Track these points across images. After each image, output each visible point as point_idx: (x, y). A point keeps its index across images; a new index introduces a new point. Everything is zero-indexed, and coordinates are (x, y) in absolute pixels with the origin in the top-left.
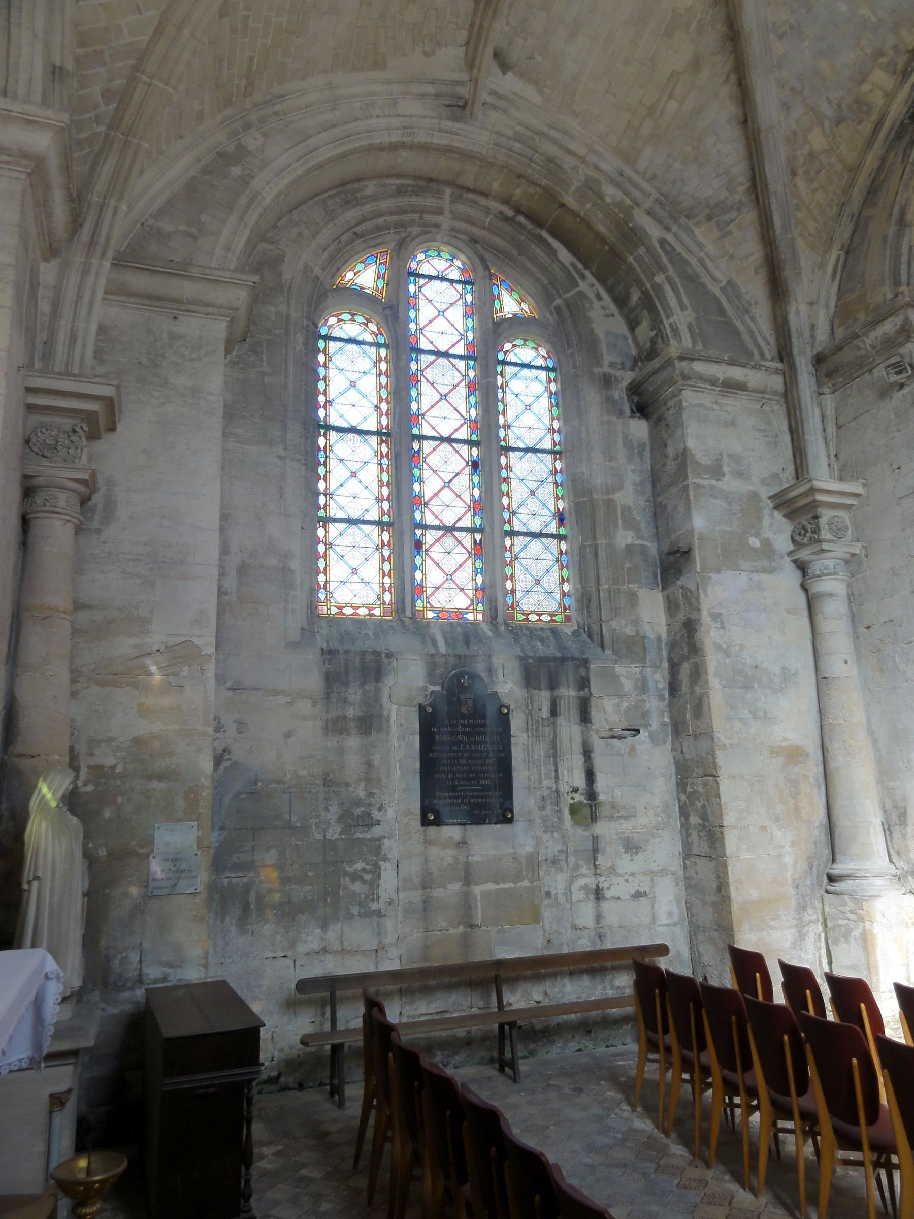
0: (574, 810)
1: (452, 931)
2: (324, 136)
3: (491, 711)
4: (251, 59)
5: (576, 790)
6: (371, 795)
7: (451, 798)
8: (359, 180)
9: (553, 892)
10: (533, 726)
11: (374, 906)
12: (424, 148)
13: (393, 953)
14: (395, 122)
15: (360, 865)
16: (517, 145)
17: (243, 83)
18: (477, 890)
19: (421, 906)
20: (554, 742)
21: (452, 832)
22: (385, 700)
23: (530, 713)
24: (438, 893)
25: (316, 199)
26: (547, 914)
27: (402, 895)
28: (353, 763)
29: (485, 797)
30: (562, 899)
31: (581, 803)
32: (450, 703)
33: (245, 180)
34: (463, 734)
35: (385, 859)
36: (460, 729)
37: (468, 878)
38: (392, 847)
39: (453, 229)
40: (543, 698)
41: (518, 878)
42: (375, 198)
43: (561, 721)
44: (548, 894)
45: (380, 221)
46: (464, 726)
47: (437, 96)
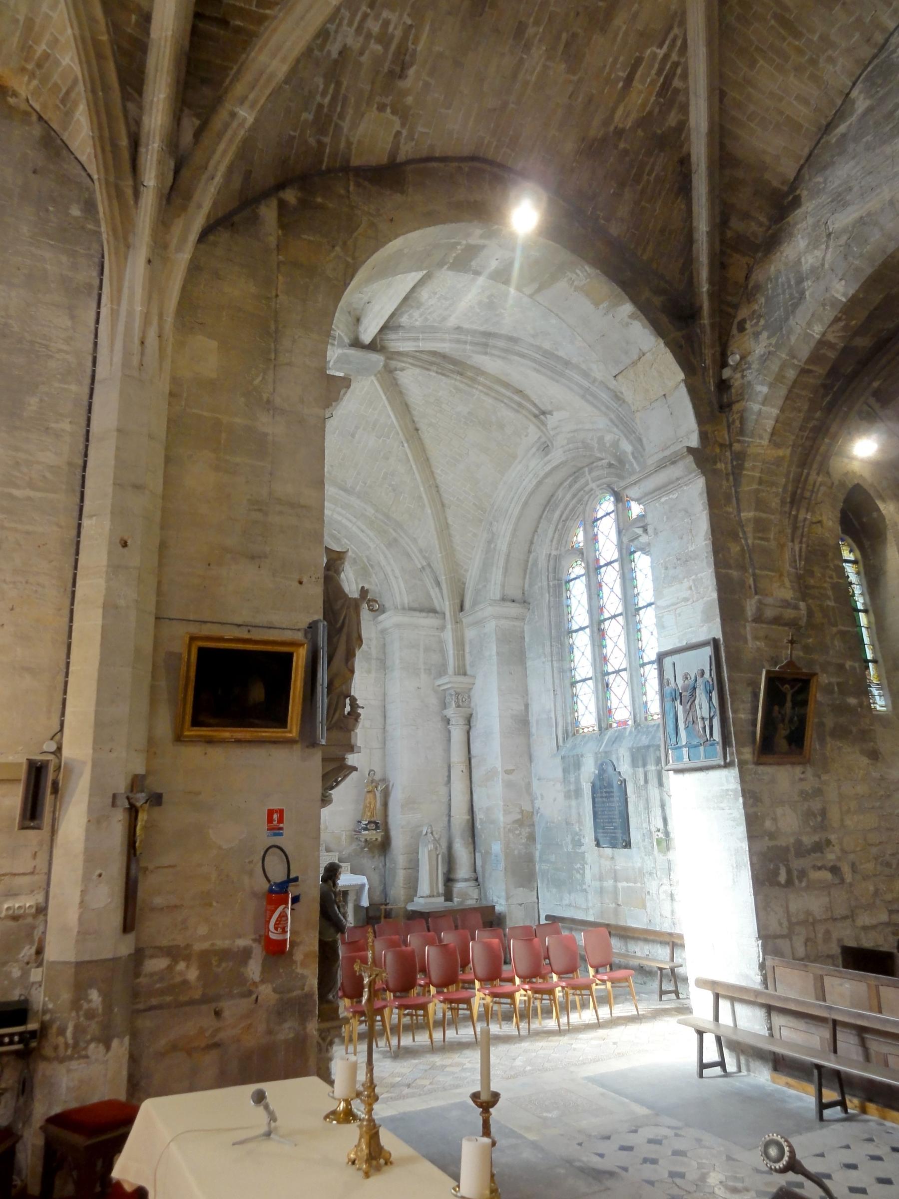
0: (659, 842)
1: (611, 905)
2: (512, 505)
3: (616, 783)
4: (474, 504)
5: (658, 830)
6: (580, 830)
7: (603, 833)
8: (552, 496)
9: (651, 892)
10: (638, 788)
11: (584, 887)
12: (547, 475)
13: (591, 912)
14: (531, 475)
15: (579, 865)
16: (571, 445)
17: (480, 511)
18: (621, 885)
19: (599, 890)
20: (647, 800)
21: (608, 851)
22: (582, 780)
23: (635, 783)
24: (605, 884)
25: (544, 517)
26: (648, 904)
27: (593, 883)
28: (574, 811)
29: (615, 833)
30: (655, 897)
31: (661, 838)
32: (600, 780)
33: (495, 549)
34: (606, 797)
35: (587, 864)
36: (604, 795)
37: (616, 880)
38: (589, 857)
39: (598, 486)
40: (641, 770)
41: (635, 882)
42: (563, 497)
43: (650, 786)
44: (649, 892)
45: (570, 506)
46: (606, 792)
47: (538, 450)
